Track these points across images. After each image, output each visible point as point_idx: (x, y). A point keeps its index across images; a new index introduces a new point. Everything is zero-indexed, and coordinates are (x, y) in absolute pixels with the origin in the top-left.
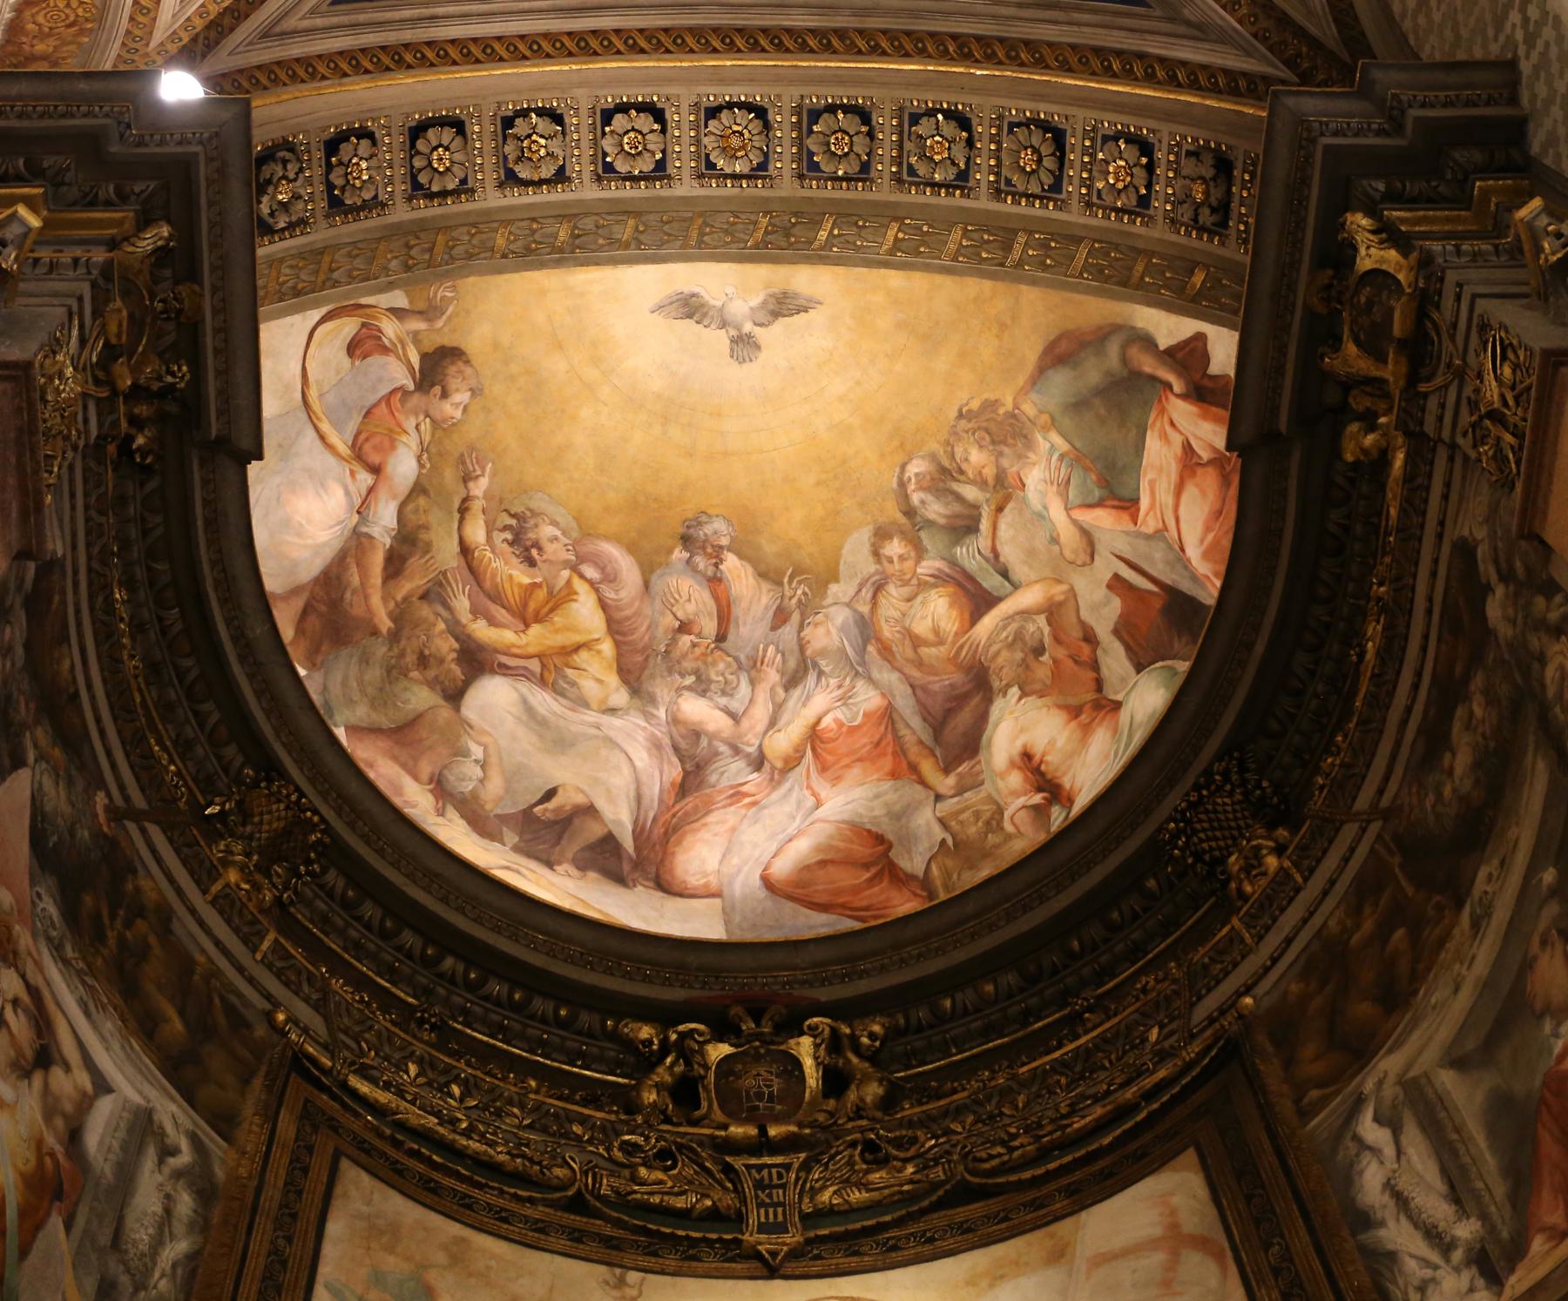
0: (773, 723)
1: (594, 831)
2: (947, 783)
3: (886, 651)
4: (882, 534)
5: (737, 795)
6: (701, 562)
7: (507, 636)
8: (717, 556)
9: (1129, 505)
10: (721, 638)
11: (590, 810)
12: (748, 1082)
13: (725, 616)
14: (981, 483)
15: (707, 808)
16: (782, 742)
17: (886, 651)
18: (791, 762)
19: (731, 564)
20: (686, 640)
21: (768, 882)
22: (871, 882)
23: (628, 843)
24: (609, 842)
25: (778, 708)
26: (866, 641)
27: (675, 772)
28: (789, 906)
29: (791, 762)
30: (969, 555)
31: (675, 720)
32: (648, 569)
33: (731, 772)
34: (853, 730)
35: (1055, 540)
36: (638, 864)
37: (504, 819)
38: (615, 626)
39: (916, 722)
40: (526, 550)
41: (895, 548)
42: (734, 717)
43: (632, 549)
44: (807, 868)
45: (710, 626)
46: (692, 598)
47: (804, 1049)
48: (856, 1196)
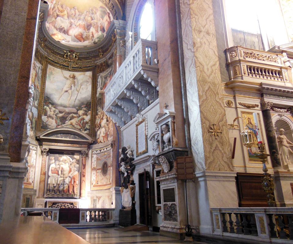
1: (64, 30)
2: (87, 32)
4: (87, 12)
8: (75, 9)
9: (103, 19)
10: (75, 15)
12: (70, 57)
13: (75, 14)
14: (94, 11)
16: (77, 24)
17: (85, 20)
18: (77, 26)
19: (76, 10)
20: (72, 15)
21: (74, 35)
22: (81, 37)
23: (66, 31)
25: (78, 22)
27: (70, 25)
28: (75, 38)
30: (92, 16)
31: (70, 21)
33: (73, 26)
35: (98, 18)
37: (58, 29)
38: (68, 13)
39: (86, 26)
41: (88, 13)
42: (75, 22)
43: (70, 8)
44: (77, 35)
45: (74, 14)
46: (73, 12)
47: (74, 54)
48: (75, 66)
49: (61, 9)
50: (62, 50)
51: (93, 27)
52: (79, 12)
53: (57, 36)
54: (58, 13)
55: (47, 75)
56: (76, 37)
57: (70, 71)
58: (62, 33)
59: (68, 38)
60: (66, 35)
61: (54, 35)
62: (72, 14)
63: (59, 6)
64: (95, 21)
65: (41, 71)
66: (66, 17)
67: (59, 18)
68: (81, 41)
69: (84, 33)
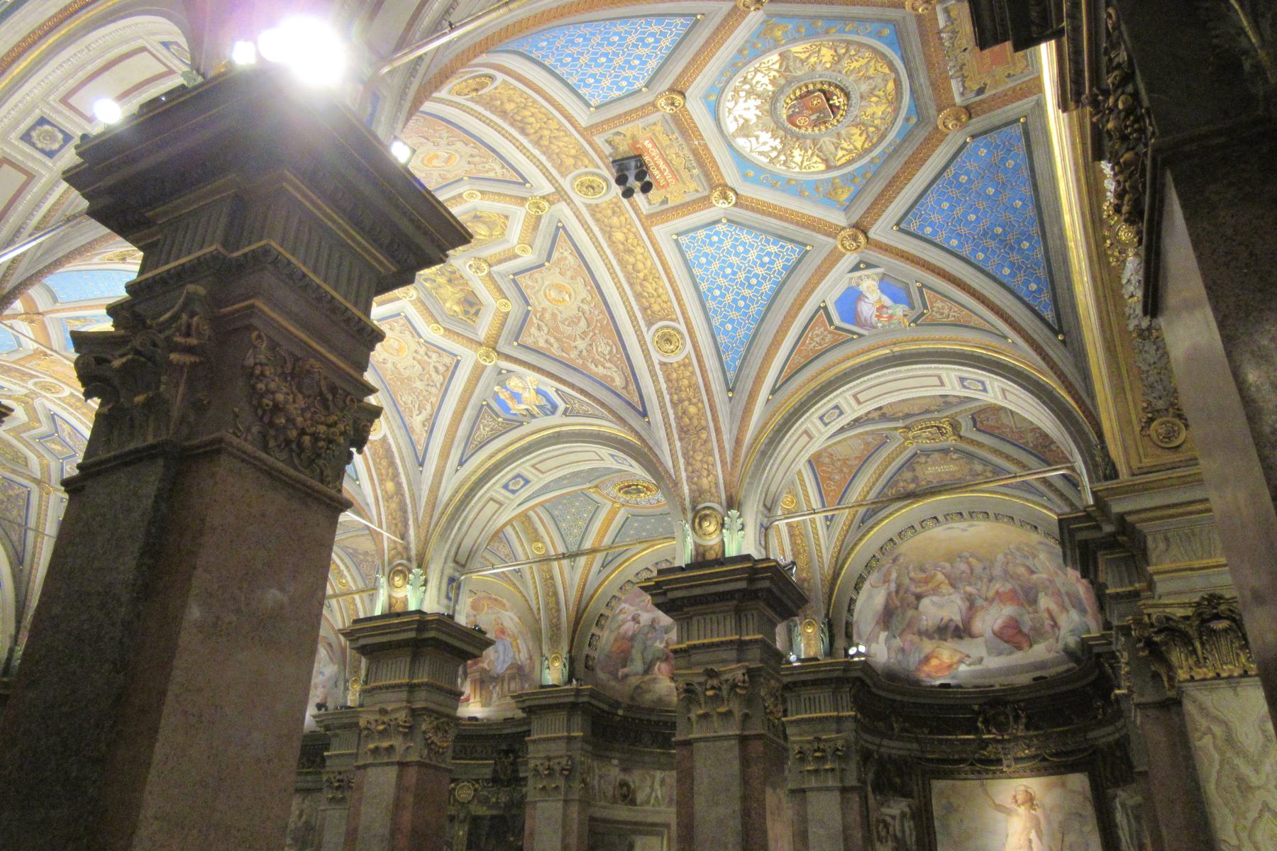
2: (1030, 609)
3: (1011, 577)
5: (983, 607)
7: (924, 588)
8: (967, 558)
11: (951, 620)
13: (972, 570)
15: (976, 611)
16: (991, 594)
17: (1011, 577)
19: (971, 559)
21: (995, 633)
24: (957, 628)
25: (988, 588)
27: (967, 604)
30: (1029, 562)
31: (965, 592)
33: (979, 602)
36: (964, 631)
37: (935, 632)
38: (947, 576)
40: (922, 570)
45: (969, 571)
46: (963, 567)
48: (1023, 755)
49: (922, 575)
50: (965, 708)
51: (1046, 594)
53: (937, 657)
54: (918, 590)
55: (937, 823)
56: (998, 635)
57: (1010, 778)
58: (950, 640)
59: (975, 649)
60: (967, 640)
61: (927, 659)
63: (912, 574)
64: (1045, 576)
65: (912, 823)
66: (946, 588)
67: (925, 602)
68: (1019, 648)
69: (1021, 615)
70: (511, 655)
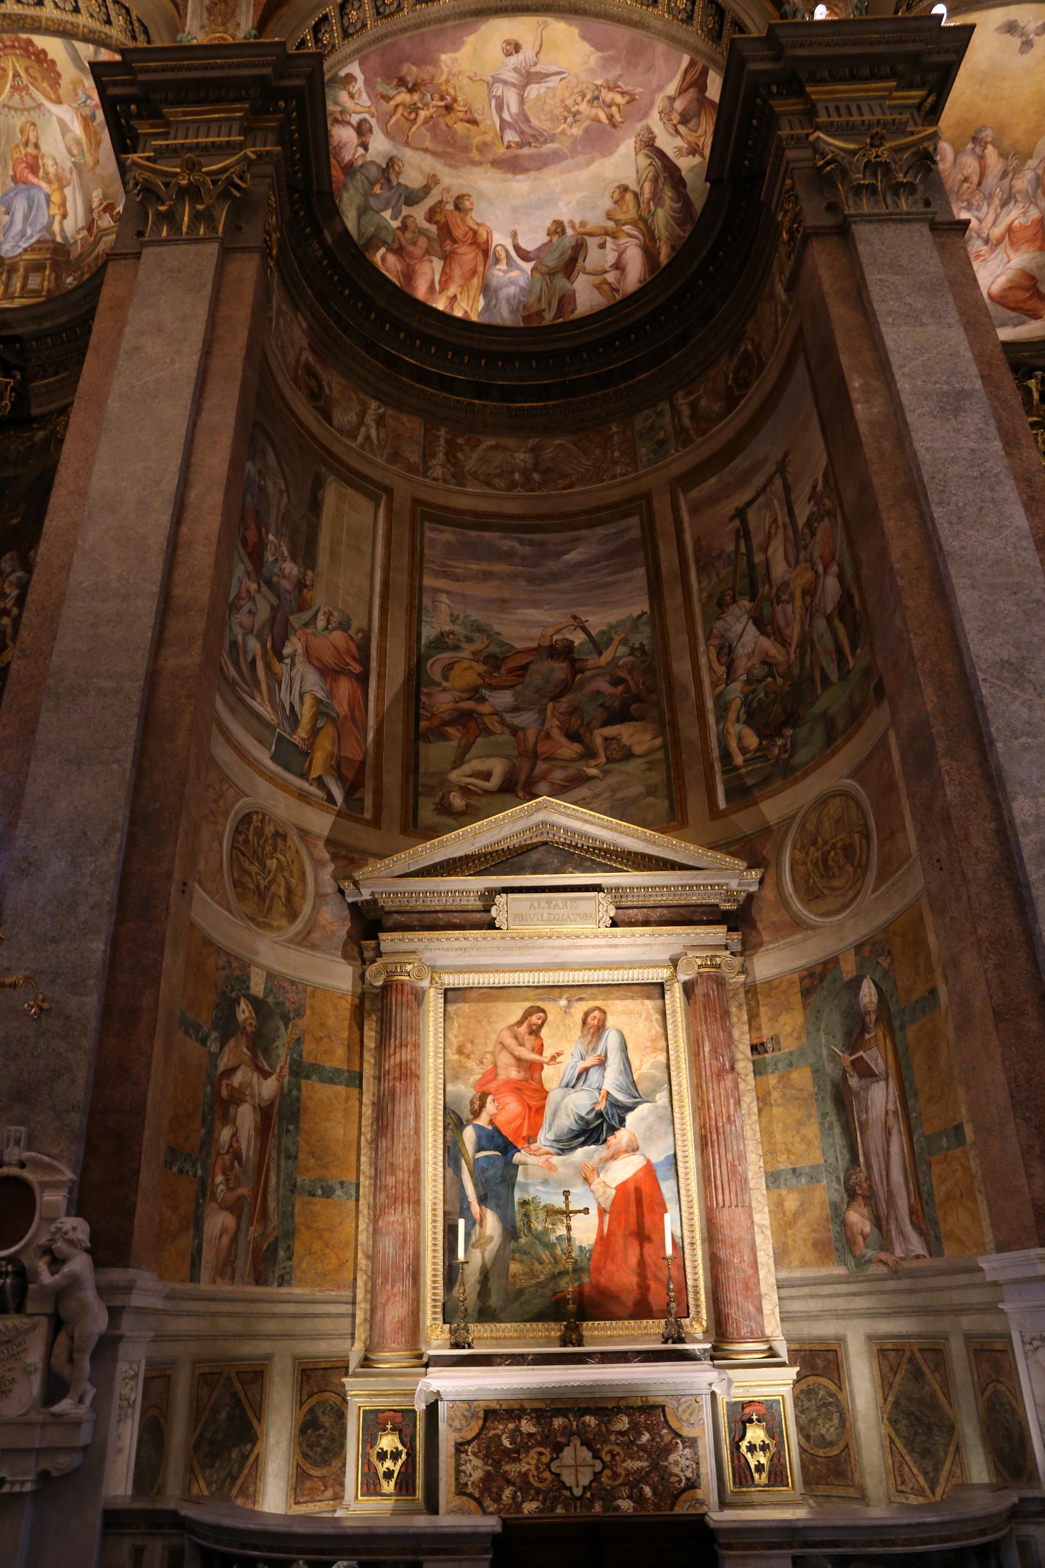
0: (994, 223)
6: (978, 149)
10: (979, 184)
13: (982, 175)
16: (997, 232)
18: (1000, 241)
19: (991, 151)
20: (966, 185)
25: (997, 216)
26: (1038, 186)
29: (1000, 241)
32: (957, 153)
34: (1026, 228)
42: (980, 220)
43: (953, 145)
45: (975, 179)
52: (1003, 155)
62: (966, 180)
70: (45, 220)
